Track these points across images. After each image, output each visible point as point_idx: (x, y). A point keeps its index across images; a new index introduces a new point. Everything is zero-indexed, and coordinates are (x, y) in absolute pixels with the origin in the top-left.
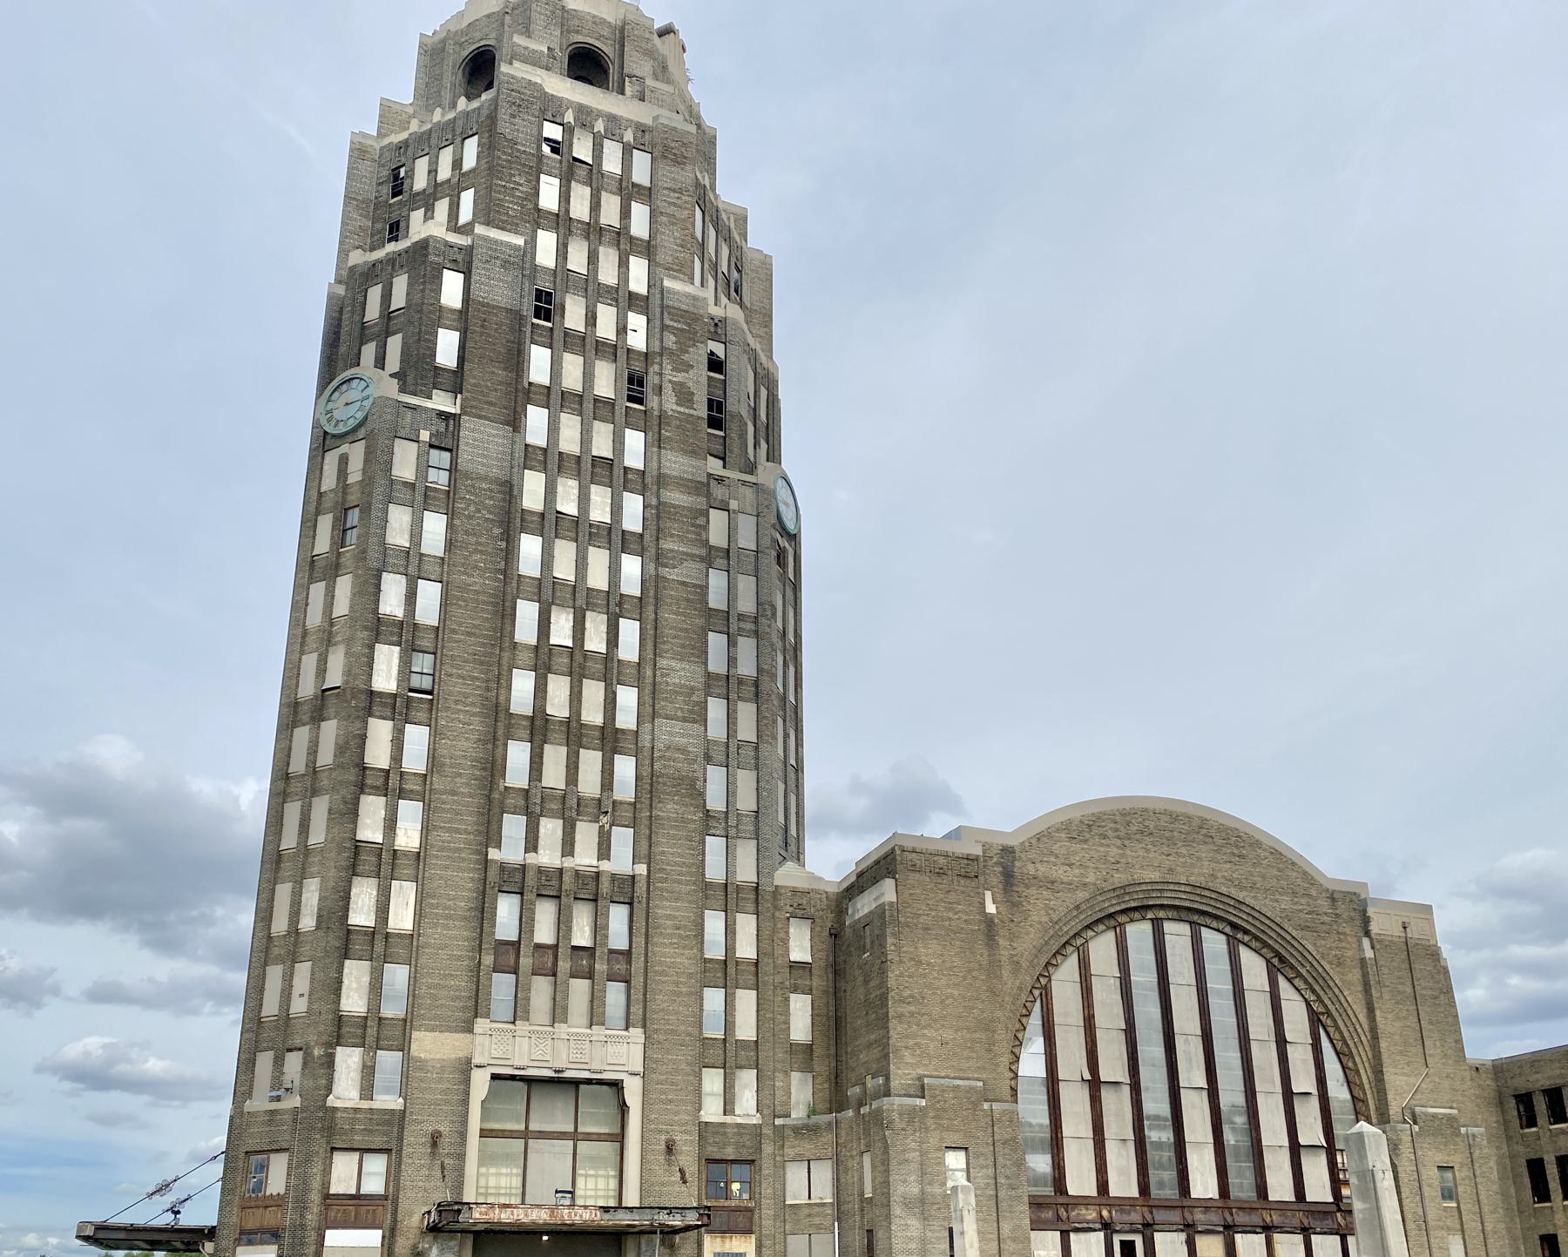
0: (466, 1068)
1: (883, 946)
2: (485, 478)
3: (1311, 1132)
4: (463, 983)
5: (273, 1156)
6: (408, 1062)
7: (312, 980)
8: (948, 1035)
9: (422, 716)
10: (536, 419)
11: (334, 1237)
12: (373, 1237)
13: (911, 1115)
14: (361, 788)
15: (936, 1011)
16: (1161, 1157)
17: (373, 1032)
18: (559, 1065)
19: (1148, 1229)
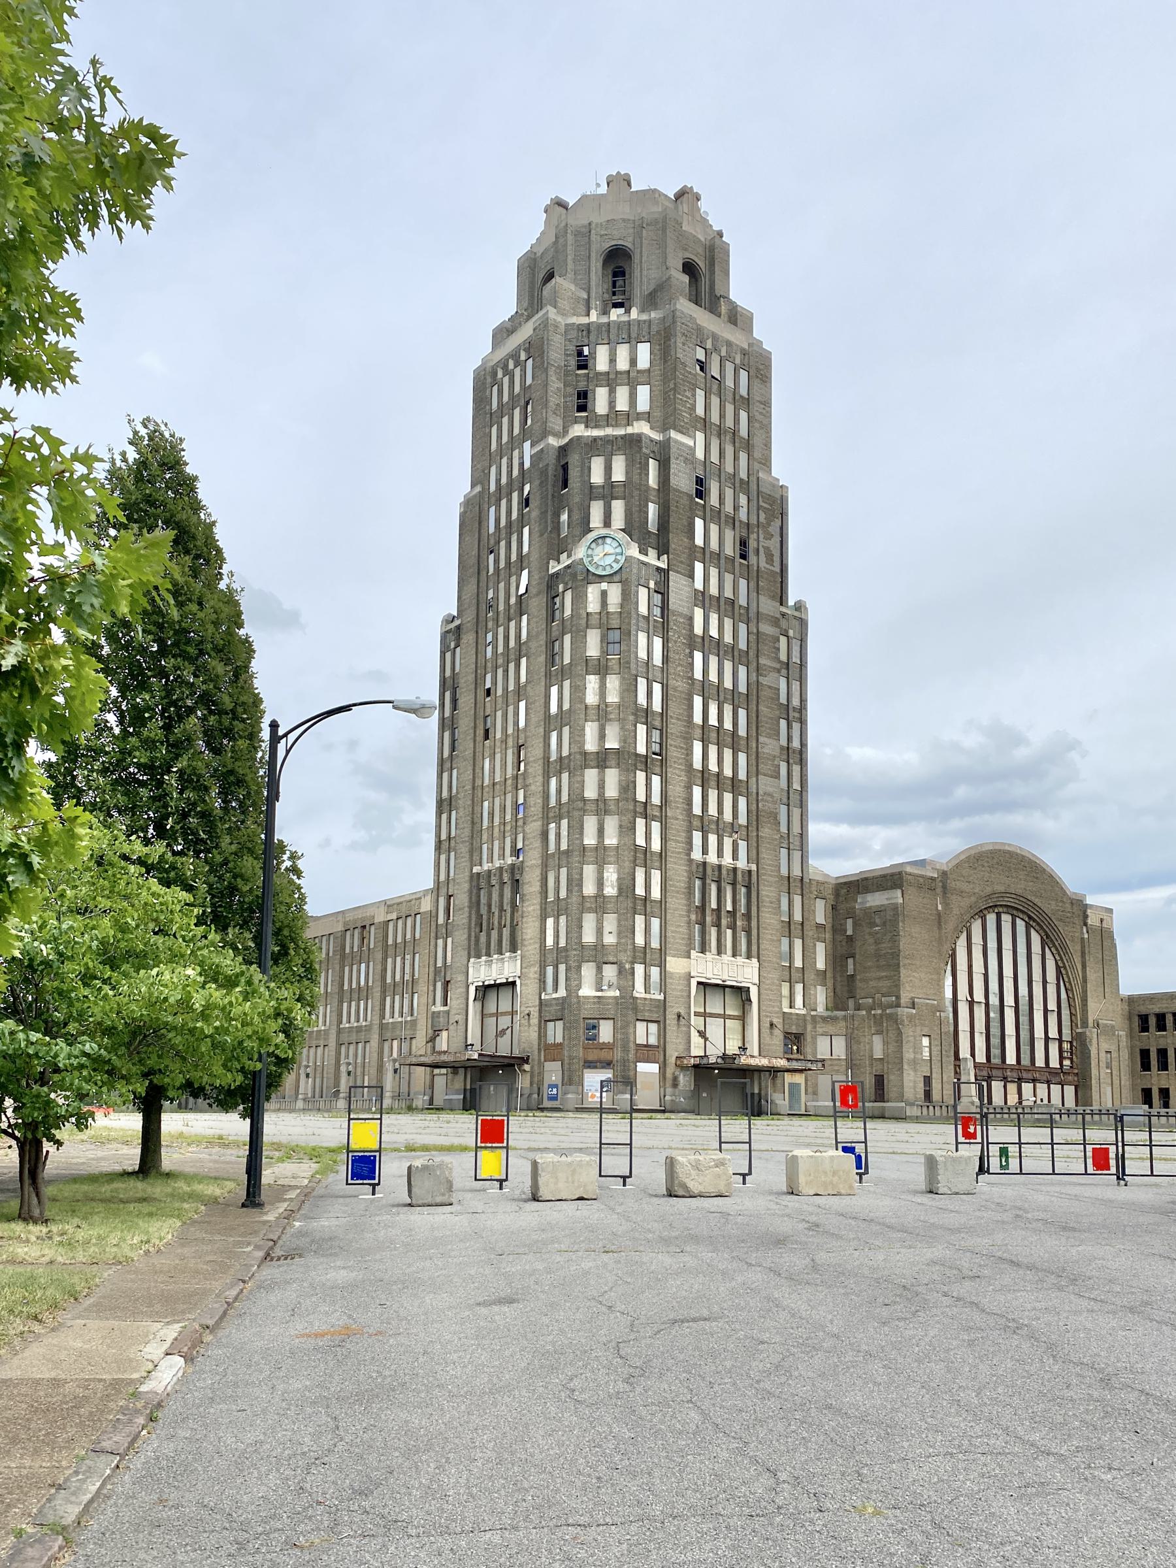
0: (689, 977)
1: (897, 926)
2: (680, 615)
3: (1053, 1033)
4: (684, 930)
5: (601, 1022)
6: (664, 974)
7: (619, 925)
8: (923, 975)
9: (658, 770)
10: (699, 567)
11: (642, 1067)
12: (654, 1068)
13: (911, 1018)
14: (635, 814)
15: (918, 963)
16: (995, 1041)
17: (643, 955)
18: (725, 977)
19: (989, 1079)
